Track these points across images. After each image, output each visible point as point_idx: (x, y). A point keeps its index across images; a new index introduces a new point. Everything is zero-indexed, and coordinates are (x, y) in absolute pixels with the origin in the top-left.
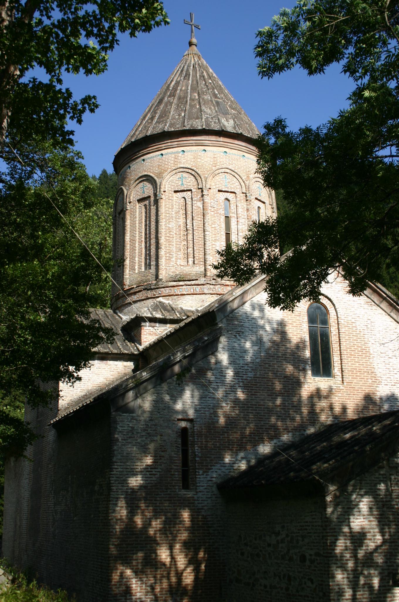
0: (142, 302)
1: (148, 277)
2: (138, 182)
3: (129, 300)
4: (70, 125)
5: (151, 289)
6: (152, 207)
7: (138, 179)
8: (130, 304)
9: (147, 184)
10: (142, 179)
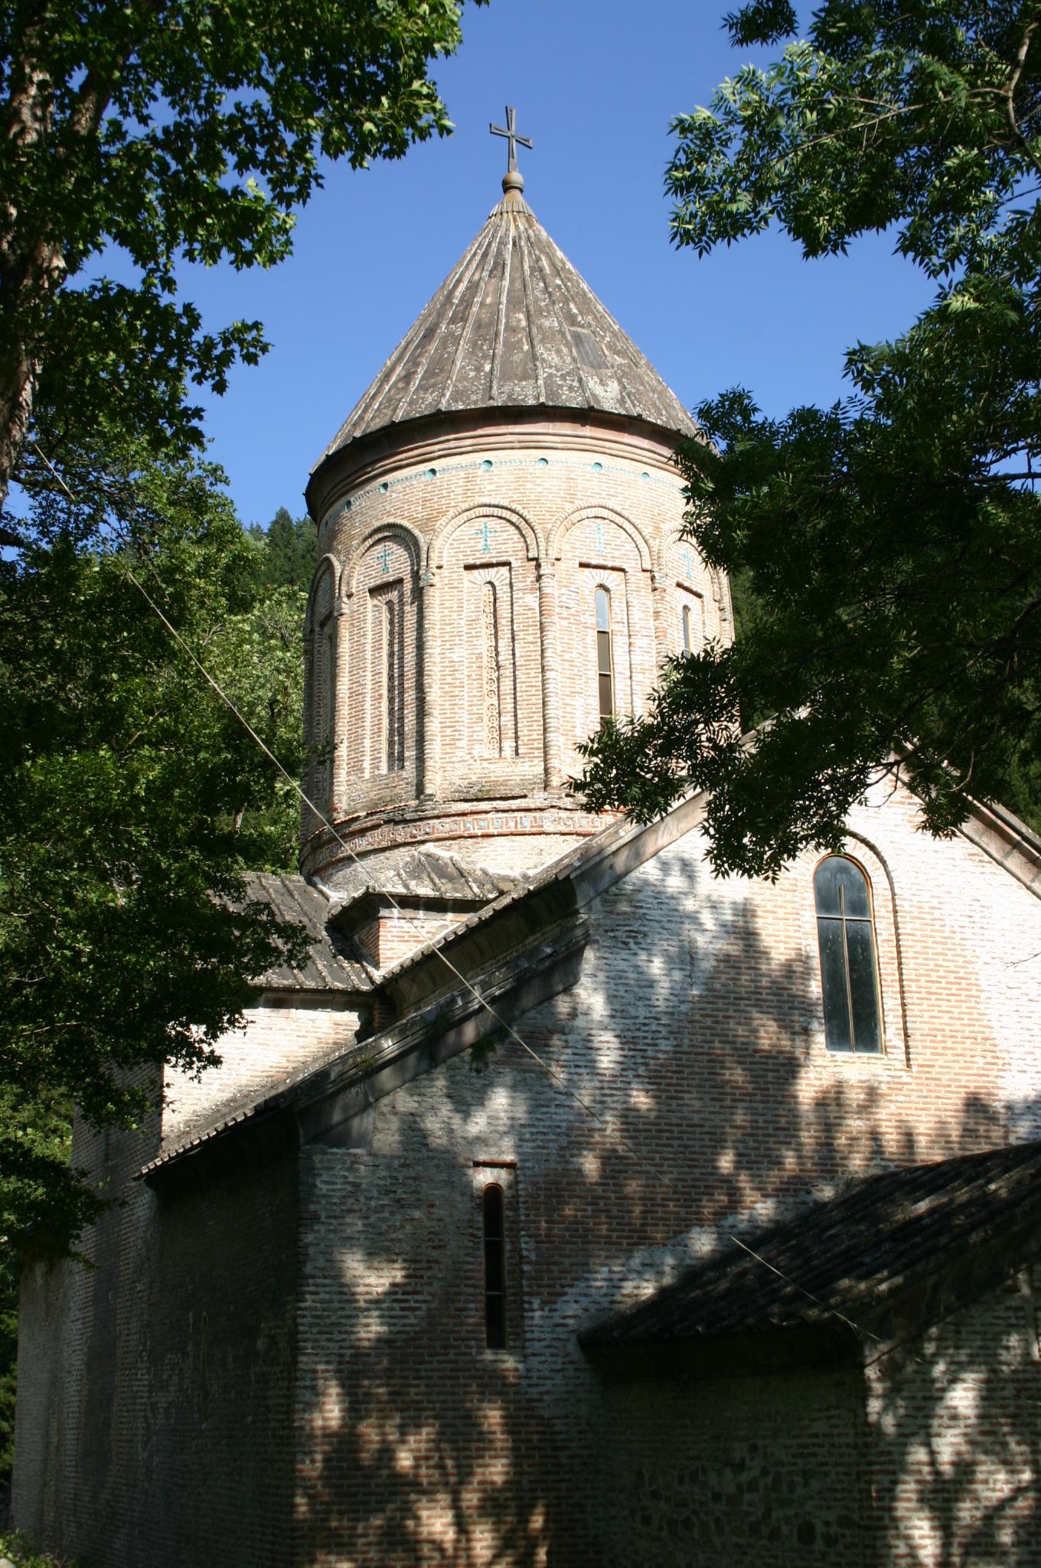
0: (382, 856)
1: (397, 790)
2: (370, 541)
3: (348, 849)
4: (195, 394)
5: (406, 822)
6: (407, 608)
7: (370, 535)
8: (350, 860)
9: (395, 547)
10: (380, 536)
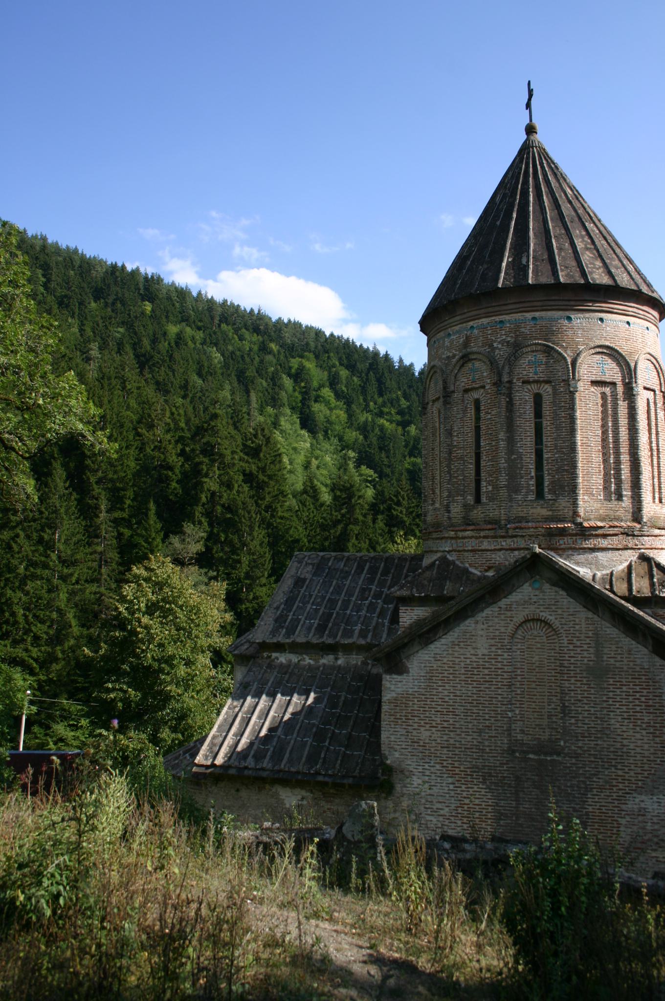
0: (617, 553)
2: (593, 351)
5: (634, 535)
6: (620, 403)
7: (594, 348)
9: (610, 361)
10: (600, 350)
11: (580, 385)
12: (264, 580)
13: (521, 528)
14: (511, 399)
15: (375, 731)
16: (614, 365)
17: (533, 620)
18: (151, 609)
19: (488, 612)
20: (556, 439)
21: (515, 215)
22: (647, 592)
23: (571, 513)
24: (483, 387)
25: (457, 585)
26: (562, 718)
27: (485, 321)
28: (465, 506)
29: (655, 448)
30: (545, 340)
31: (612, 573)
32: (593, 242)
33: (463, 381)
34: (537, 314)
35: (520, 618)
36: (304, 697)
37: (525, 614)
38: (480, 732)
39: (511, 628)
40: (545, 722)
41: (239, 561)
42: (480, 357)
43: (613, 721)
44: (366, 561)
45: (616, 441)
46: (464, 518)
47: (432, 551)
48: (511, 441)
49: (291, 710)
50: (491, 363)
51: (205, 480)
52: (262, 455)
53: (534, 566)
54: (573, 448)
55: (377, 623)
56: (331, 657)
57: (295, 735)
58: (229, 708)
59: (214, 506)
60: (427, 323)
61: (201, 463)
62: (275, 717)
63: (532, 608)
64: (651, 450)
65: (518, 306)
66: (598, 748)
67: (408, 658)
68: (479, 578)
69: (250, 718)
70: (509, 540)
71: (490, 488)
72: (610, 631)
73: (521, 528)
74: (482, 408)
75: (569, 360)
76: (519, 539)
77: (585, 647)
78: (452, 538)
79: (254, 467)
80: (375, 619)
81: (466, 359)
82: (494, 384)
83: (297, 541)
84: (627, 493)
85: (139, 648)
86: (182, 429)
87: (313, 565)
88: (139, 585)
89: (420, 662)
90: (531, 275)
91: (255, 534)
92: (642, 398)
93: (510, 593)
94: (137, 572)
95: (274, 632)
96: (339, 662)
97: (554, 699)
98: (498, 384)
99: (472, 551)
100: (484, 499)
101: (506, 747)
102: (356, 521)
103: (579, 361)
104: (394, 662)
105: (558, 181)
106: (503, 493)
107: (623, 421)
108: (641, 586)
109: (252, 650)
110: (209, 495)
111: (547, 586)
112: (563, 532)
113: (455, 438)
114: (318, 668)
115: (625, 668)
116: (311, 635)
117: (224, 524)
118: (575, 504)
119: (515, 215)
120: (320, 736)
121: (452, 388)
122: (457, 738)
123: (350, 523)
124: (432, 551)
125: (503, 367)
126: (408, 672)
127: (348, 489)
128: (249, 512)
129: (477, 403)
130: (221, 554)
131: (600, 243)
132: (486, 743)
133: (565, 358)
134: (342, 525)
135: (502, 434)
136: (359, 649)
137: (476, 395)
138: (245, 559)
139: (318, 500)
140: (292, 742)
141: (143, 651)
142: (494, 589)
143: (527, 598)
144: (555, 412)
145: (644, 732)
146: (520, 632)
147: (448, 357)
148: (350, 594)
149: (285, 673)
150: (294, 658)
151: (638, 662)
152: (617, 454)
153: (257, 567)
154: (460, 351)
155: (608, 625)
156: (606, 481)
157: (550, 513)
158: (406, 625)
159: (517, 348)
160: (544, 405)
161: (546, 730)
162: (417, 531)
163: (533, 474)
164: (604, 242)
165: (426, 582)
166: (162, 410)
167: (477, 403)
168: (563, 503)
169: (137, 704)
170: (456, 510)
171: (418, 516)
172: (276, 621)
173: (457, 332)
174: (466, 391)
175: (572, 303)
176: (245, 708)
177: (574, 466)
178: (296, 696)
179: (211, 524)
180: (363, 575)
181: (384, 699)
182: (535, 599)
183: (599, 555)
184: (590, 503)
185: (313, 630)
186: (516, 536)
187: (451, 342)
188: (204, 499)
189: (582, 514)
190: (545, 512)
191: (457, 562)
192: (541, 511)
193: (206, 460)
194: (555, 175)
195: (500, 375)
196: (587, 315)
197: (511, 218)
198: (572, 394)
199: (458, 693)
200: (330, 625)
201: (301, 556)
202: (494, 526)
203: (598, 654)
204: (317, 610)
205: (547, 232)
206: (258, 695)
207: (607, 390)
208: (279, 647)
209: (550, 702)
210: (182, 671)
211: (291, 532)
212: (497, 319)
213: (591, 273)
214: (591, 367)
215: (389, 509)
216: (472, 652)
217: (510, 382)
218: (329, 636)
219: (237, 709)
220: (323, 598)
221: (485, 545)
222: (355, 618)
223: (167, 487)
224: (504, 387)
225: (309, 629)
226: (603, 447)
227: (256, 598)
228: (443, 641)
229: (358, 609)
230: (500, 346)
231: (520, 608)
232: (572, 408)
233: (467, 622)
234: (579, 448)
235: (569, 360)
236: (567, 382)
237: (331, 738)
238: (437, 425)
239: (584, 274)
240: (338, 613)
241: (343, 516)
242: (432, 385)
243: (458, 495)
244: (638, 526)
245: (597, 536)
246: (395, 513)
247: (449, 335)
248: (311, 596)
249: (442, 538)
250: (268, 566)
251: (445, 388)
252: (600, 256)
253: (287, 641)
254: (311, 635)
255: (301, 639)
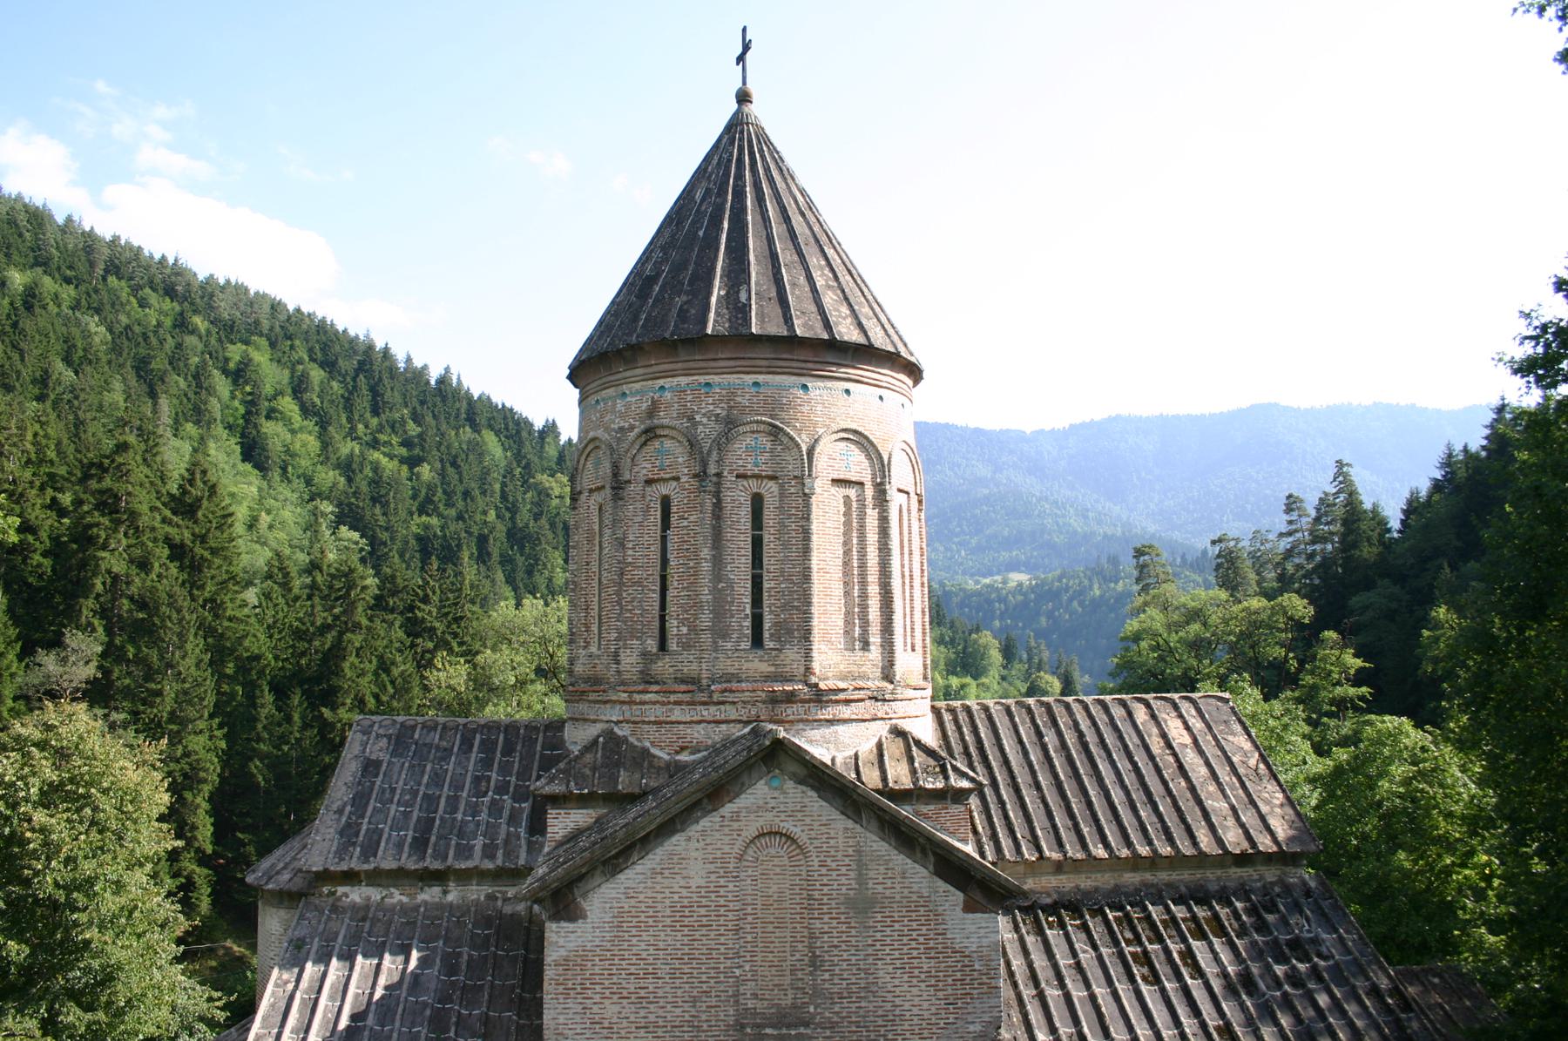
3: (828, 713)
6: (869, 511)
8: (831, 722)
11: (818, 484)
12: (201, 725)
13: (731, 691)
14: (719, 501)
15: (537, 1008)
16: (862, 457)
17: (770, 833)
18: (48, 797)
19: (705, 823)
20: (782, 562)
21: (726, 225)
22: (906, 783)
23: (802, 669)
24: (677, 479)
25: (637, 776)
26: (811, 973)
27: (684, 380)
28: (645, 654)
29: (907, 574)
30: (772, 417)
31: (856, 755)
32: (836, 278)
33: (645, 468)
34: (760, 378)
35: (752, 831)
36: (401, 958)
37: (758, 825)
38: (694, 1001)
39: (739, 844)
40: (787, 980)
41: (159, 693)
42: (673, 433)
43: (881, 973)
44: (474, 731)
45: (863, 566)
46: (641, 672)
47: (585, 720)
48: (718, 562)
49: (382, 981)
50: (691, 445)
51: (104, 554)
52: (200, 514)
53: (777, 756)
54: (806, 577)
55: (508, 834)
56: (436, 890)
57: (397, 1024)
58: (276, 985)
59: (114, 599)
60: (587, 369)
61: (98, 525)
62: (357, 996)
63: (769, 816)
64: (903, 576)
65: (732, 363)
66: (862, 1012)
67: (584, 895)
68: (668, 764)
69: (317, 1000)
70: (713, 709)
71: (685, 630)
72: (878, 845)
73: (731, 691)
74: (674, 509)
75: (804, 448)
76: (728, 707)
77: (844, 869)
78: (623, 703)
79: (187, 534)
80: (504, 827)
81: (650, 434)
82: (695, 476)
83: (257, 658)
84: (875, 639)
85: (30, 867)
86: (52, 462)
87: (389, 737)
88: (27, 756)
89: (603, 901)
90: (754, 320)
91: (189, 646)
92: (896, 500)
93: (737, 795)
94: (23, 731)
95: (341, 853)
96: (450, 897)
97: (800, 946)
98: (701, 476)
99: (655, 723)
100: (673, 645)
101: (731, 1020)
102: (358, 626)
103: (818, 450)
104: (562, 900)
105: (785, 179)
106: (706, 638)
107: (872, 537)
108: (899, 775)
109: (299, 884)
110: (109, 581)
111: (790, 784)
112: (790, 698)
113: (630, 552)
114: (416, 908)
115: (898, 898)
116: (405, 856)
117: (135, 629)
118: (808, 656)
119: (726, 225)
120: (438, 1022)
121: (627, 476)
122: (661, 1012)
123: (348, 630)
124: (585, 720)
125: (709, 452)
126: (585, 917)
127: (346, 575)
128: (179, 611)
129: (666, 503)
130: (127, 681)
131: (845, 279)
132: (704, 1017)
133: (798, 446)
134: (334, 633)
135: (706, 551)
136: (480, 875)
137: (664, 490)
138: (170, 689)
139: (290, 590)
140: (395, 1035)
141: (37, 873)
142: (717, 790)
143: (761, 802)
144: (781, 523)
145: (923, 985)
146: (750, 851)
147: (621, 429)
148: (457, 786)
149: (364, 919)
150: (375, 894)
151: (915, 888)
152: (864, 584)
153: (190, 703)
154: (642, 422)
155: (875, 838)
156: (848, 622)
157: (772, 669)
158: (558, 837)
159: (730, 425)
160: (766, 512)
161: (790, 992)
162: (455, 644)
163: (748, 611)
164: (848, 278)
165: (587, 772)
166: (18, 428)
167: (666, 503)
168: (791, 655)
169: (20, 967)
170: (630, 661)
171: (457, 620)
172: (341, 833)
173: (637, 392)
174: (649, 482)
175: (810, 365)
176: (304, 984)
177: (807, 601)
178: (387, 956)
179: (109, 631)
180: (474, 755)
181: (548, 960)
182: (773, 803)
183: (840, 728)
184: (830, 658)
185: (406, 849)
186: (723, 703)
187: (628, 406)
188: (99, 587)
189: (817, 671)
190: (765, 668)
191: (631, 739)
192: (757, 665)
193: (105, 521)
194: (781, 170)
195: (704, 464)
196: (829, 384)
197: (719, 229)
198: (807, 497)
199: (661, 945)
200: (433, 839)
201: (367, 723)
202: (691, 687)
203: (861, 880)
204: (407, 815)
205: (774, 257)
206: (324, 959)
207: (852, 492)
208: (350, 877)
209: (794, 951)
210: (110, 903)
211: (246, 643)
212: (702, 379)
213: (837, 324)
214: (834, 460)
215: (411, 608)
216: (683, 883)
217: (719, 475)
218: (435, 857)
219: (290, 986)
220: (415, 793)
221: (677, 714)
222: (472, 826)
223: (24, 561)
224: (707, 479)
225: (400, 846)
226: (845, 574)
227: (186, 754)
228: (638, 868)
229: (474, 810)
230: (705, 420)
231: (752, 816)
232: (807, 518)
233: (674, 839)
234: (815, 576)
235: (804, 448)
236: (800, 479)
237: (457, 1024)
238: (596, 527)
239: (827, 325)
240: (442, 819)
241: (336, 618)
242: (589, 465)
243: (633, 637)
244: (891, 687)
245: (837, 702)
246: (419, 614)
247: (624, 394)
248: (393, 790)
249: (605, 702)
250: (210, 700)
251: (615, 475)
252: (846, 299)
253: (366, 867)
254: (405, 856)
255: (389, 864)
